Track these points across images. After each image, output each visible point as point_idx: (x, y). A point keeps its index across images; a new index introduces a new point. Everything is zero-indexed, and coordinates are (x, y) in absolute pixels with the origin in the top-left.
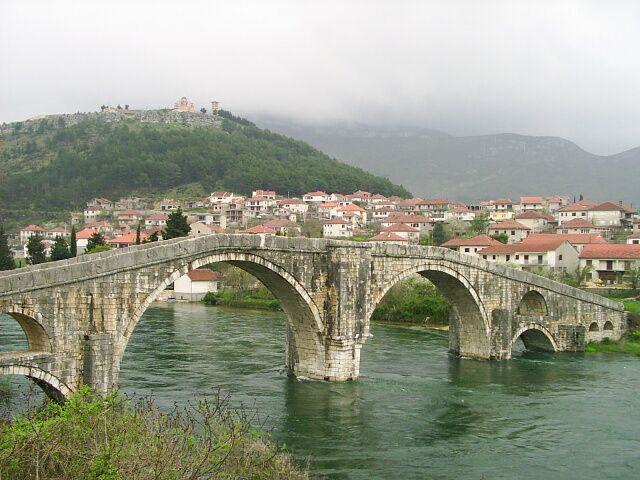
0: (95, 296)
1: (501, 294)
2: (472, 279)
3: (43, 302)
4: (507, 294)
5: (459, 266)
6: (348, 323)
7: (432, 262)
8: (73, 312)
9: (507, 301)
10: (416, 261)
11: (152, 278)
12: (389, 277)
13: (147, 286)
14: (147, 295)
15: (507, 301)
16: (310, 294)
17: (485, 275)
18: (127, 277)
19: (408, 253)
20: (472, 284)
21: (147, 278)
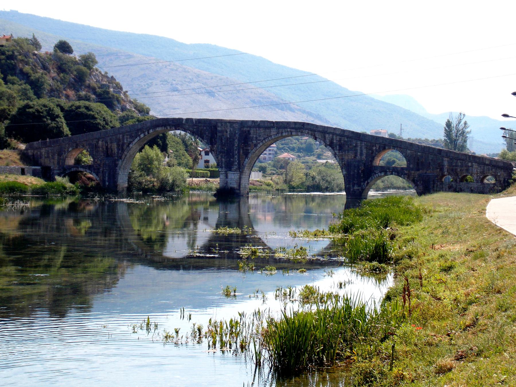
0: (109, 143)
1: (356, 150)
2: (328, 141)
3: (90, 144)
4: (361, 151)
5: (316, 133)
6: (222, 161)
7: (292, 130)
8: (101, 149)
9: (361, 154)
10: (280, 130)
11: (131, 137)
12: (261, 138)
13: (129, 140)
14: (129, 144)
15: (361, 154)
16: (210, 146)
17: (340, 138)
18: (121, 136)
19: (275, 125)
20: (328, 144)
21: (129, 136)
